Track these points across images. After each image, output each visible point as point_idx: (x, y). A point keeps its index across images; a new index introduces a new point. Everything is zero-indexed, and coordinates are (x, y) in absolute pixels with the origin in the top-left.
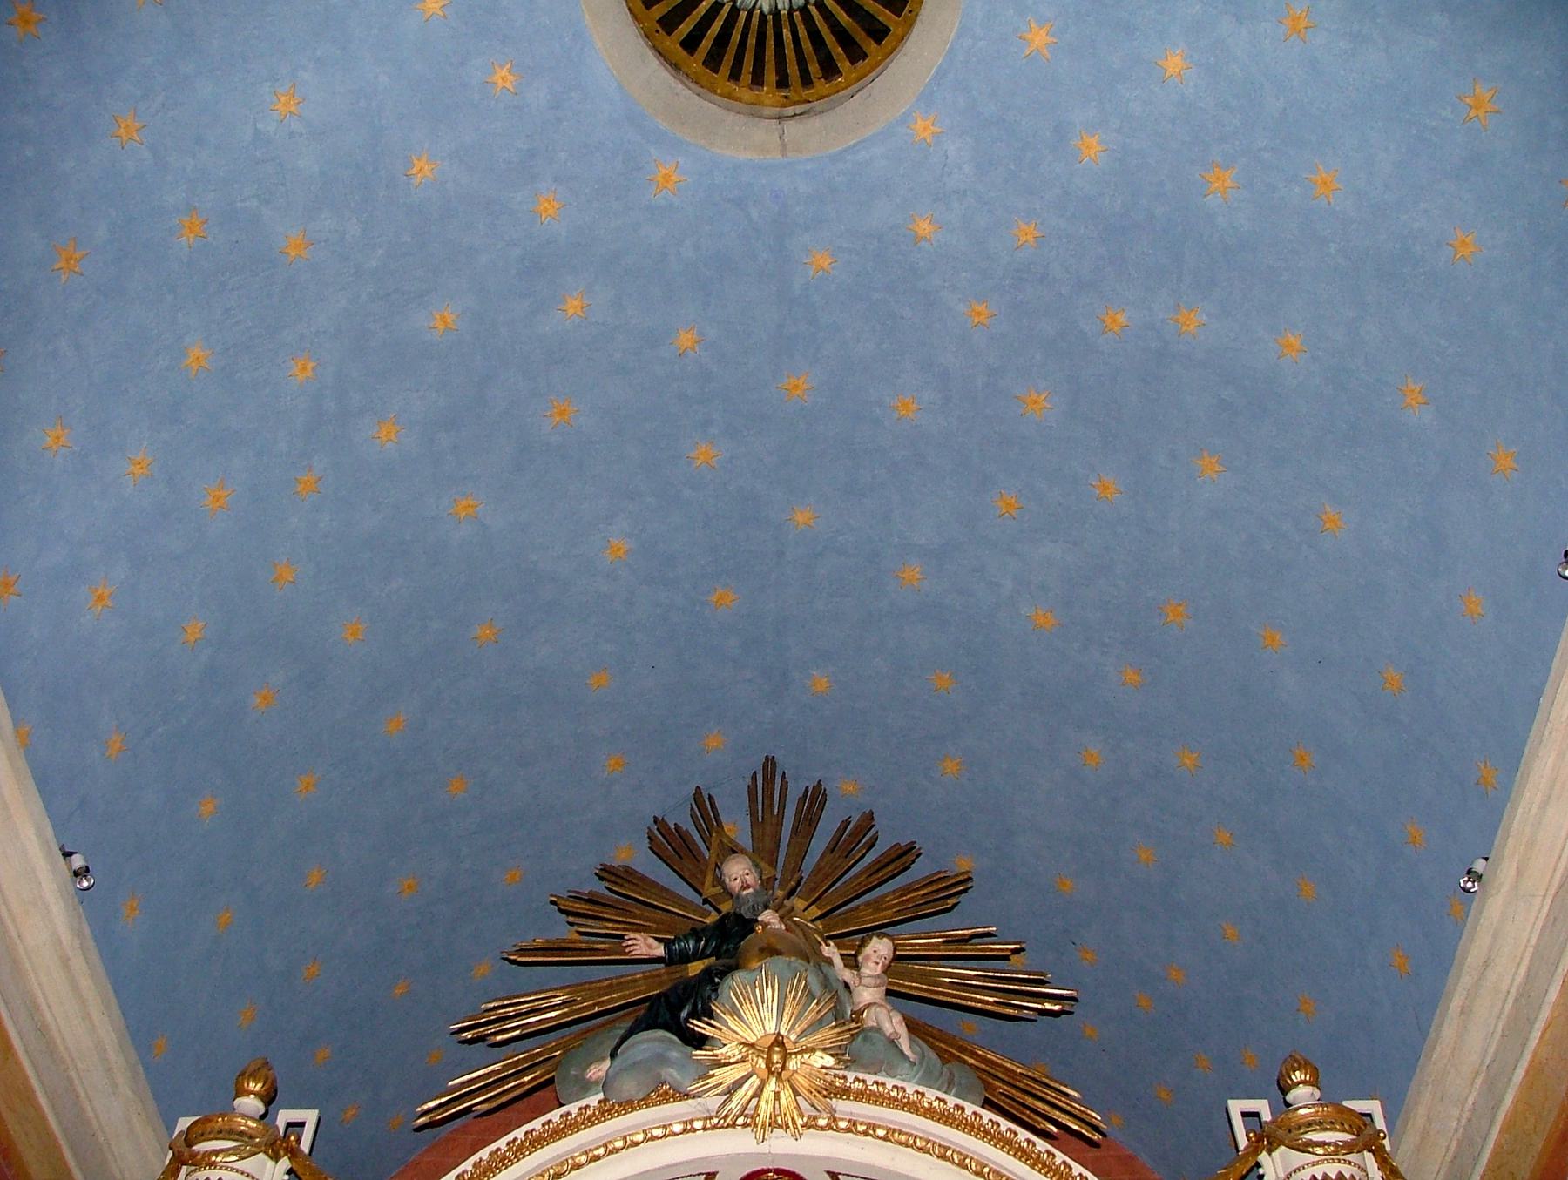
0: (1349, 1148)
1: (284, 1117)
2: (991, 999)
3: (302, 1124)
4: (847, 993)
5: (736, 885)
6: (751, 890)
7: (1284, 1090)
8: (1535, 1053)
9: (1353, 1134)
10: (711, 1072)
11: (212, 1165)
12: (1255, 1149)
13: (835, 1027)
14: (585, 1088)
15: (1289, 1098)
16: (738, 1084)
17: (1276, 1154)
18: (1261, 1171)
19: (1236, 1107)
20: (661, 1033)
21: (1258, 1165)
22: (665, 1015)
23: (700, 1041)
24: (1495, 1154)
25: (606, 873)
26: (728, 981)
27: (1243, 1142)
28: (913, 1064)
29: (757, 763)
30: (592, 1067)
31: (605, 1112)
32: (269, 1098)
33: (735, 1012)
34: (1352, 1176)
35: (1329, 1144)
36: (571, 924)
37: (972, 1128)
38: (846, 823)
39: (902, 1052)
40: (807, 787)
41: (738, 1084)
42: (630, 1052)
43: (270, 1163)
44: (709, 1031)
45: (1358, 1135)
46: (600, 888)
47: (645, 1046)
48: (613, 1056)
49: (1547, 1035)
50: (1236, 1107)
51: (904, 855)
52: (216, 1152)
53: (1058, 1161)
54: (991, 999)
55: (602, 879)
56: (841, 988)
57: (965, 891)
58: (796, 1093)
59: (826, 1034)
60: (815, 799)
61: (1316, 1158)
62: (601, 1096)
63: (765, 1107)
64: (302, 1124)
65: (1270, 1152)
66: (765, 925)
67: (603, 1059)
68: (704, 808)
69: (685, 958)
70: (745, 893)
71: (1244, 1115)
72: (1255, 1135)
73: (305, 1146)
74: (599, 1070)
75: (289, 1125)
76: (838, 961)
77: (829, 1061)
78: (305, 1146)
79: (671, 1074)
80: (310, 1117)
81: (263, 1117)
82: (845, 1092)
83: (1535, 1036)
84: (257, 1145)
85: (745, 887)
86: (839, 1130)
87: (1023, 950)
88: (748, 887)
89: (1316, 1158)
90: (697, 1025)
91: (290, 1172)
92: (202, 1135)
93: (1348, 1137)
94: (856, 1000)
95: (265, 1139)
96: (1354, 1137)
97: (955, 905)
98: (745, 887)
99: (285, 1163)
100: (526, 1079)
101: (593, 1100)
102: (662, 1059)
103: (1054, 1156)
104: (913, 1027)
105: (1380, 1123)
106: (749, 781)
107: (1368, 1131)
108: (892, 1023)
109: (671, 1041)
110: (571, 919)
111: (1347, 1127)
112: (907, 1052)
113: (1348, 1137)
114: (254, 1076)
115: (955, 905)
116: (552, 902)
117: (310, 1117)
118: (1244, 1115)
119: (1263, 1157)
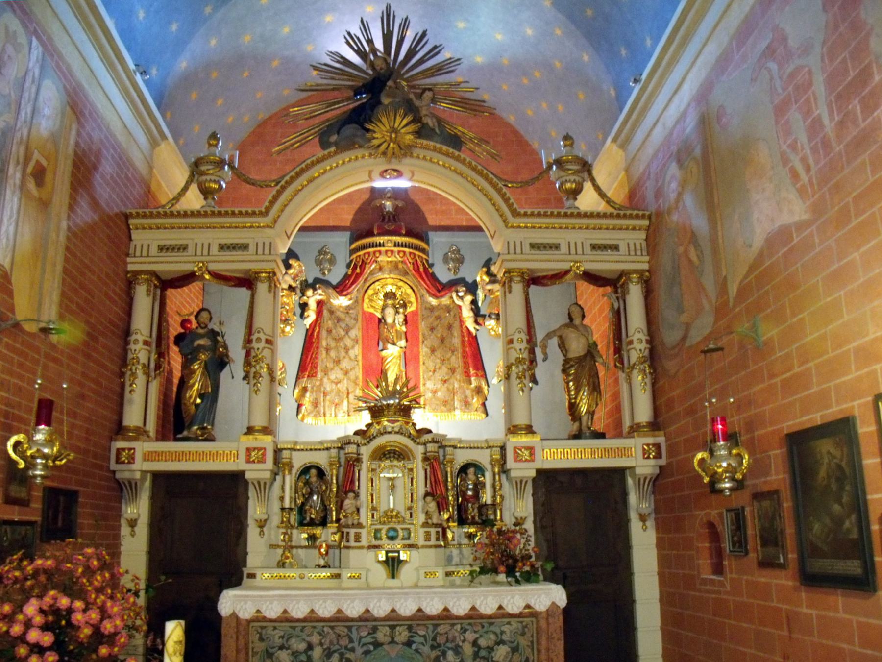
11: (208, 174)
16: (379, 146)
23: (368, 130)
41: (379, 146)
44: (371, 128)
48: (338, 133)
52: (208, 170)
63: (390, 151)
77: (412, 137)
90: (367, 126)
98: (381, 69)
102: (355, 136)
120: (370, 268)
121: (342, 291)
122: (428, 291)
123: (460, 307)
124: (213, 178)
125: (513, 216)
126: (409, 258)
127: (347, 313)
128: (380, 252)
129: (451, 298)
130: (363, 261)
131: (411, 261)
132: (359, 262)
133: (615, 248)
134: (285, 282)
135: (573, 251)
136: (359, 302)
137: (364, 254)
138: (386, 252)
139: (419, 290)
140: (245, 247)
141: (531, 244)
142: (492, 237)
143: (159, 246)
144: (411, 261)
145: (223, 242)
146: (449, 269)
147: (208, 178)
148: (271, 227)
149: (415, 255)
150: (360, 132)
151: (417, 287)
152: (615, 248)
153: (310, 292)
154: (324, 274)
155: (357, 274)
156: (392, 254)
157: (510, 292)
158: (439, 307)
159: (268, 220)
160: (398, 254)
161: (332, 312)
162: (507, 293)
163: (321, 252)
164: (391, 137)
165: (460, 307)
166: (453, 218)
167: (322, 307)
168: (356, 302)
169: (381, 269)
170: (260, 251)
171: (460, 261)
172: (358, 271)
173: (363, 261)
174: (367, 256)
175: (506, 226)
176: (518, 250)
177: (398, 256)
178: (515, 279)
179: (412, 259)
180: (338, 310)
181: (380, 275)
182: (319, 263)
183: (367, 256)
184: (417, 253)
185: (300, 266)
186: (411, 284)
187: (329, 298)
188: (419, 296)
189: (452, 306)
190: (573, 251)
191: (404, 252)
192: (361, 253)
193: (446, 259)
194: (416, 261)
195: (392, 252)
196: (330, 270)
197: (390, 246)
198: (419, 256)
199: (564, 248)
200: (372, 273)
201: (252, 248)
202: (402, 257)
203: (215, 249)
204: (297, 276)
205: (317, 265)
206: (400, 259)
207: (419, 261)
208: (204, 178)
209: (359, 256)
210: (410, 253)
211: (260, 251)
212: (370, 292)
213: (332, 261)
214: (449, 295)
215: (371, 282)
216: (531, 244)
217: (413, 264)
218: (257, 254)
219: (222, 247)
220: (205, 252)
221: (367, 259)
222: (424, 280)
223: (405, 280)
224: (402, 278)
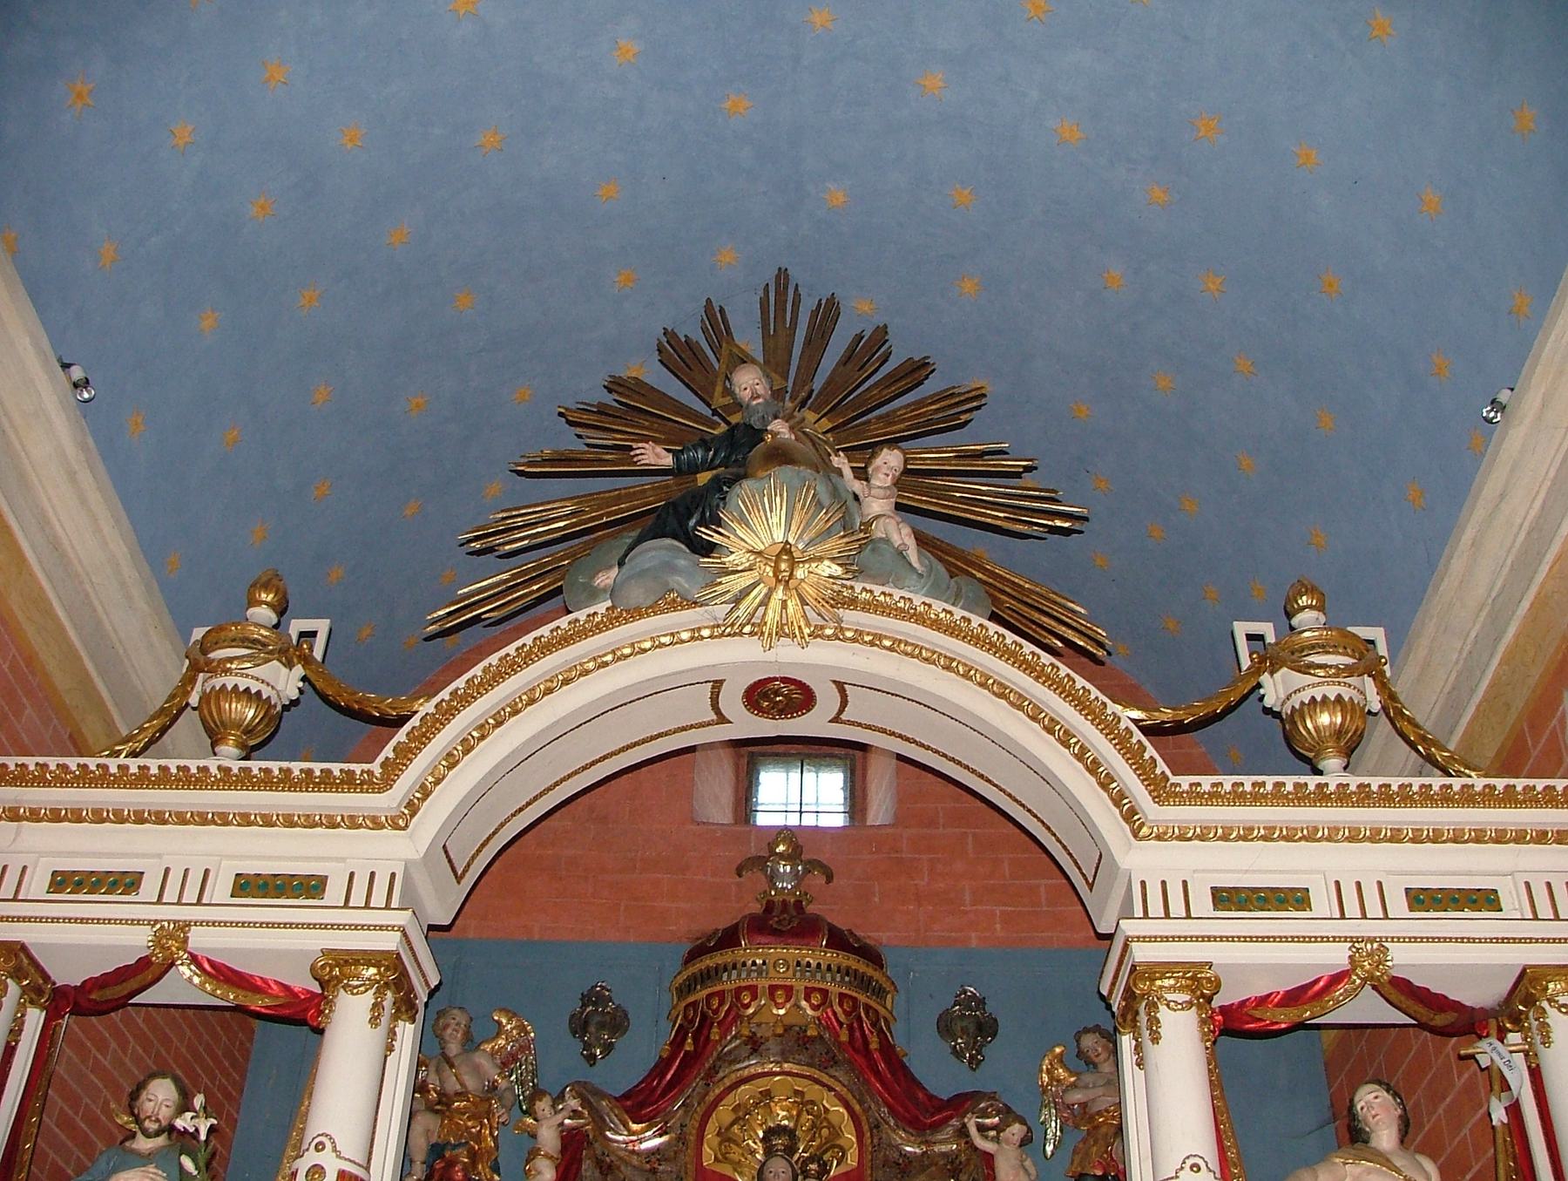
0: (1350, 671)
1: (296, 626)
2: (1002, 515)
3: (313, 634)
4: (856, 504)
5: (746, 395)
6: (760, 400)
7: (1289, 616)
8: (1543, 585)
9: (1355, 658)
10: (719, 580)
11: (227, 671)
12: (1257, 670)
13: (844, 537)
14: (593, 595)
15: (1295, 621)
16: (746, 592)
17: (1277, 675)
18: (1262, 691)
19: (1241, 629)
20: (668, 541)
21: (1259, 686)
22: (672, 523)
23: (708, 549)
24: (1492, 686)
25: (616, 384)
26: (737, 489)
27: (1246, 663)
28: (921, 576)
29: (769, 275)
30: (600, 575)
31: (612, 620)
32: (282, 609)
33: (743, 521)
34: (1351, 698)
35: (1331, 667)
36: (579, 436)
37: (978, 640)
38: (860, 337)
39: (910, 564)
40: (820, 300)
41: (746, 592)
42: (638, 560)
43: (284, 670)
44: (716, 539)
45: (1360, 659)
46: (609, 399)
47: (653, 553)
48: (621, 564)
49: (1555, 568)
50: (1241, 629)
51: (917, 371)
52: (231, 660)
53: (1062, 674)
54: (1002, 515)
55: (610, 391)
56: (851, 497)
57: (978, 408)
58: (804, 602)
59: (834, 544)
60: (828, 313)
61: (1318, 680)
62: (609, 603)
63: (772, 615)
64: (313, 634)
65: (1272, 674)
66: (774, 434)
67: (611, 567)
68: (716, 321)
69: (694, 468)
70: (755, 403)
71: (1250, 637)
72: (1259, 657)
73: (318, 654)
74: (606, 579)
75: (302, 635)
76: (848, 472)
77: (837, 570)
78: (318, 654)
79: (679, 581)
80: (322, 626)
81: (276, 626)
82: (852, 603)
83: (1544, 569)
84: (271, 652)
85: (755, 396)
86: (845, 639)
87: (1036, 468)
88: (758, 397)
89: (1318, 680)
90: (705, 533)
91: (304, 679)
92: (216, 643)
93: (1350, 661)
94: (866, 510)
95: (278, 647)
96: (1356, 661)
97: (967, 423)
98: (755, 396)
99: (299, 671)
100: (535, 588)
101: (601, 607)
102: (672, 569)
103: (1058, 669)
104: (922, 541)
105: (1382, 649)
106: (761, 293)
107: (1369, 656)
108: (900, 534)
109: (681, 550)
110: (579, 431)
111: (1349, 651)
112: (916, 564)
113: (1350, 661)
114: (266, 587)
115: (967, 423)
116: (561, 414)
117: (322, 626)
118: (1250, 637)
119: (1265, 678)
120: (723, 1036)
121: (642, 1105)
122: (892, 1111)
123: (988, 1158)
124: (243, 683)
125: (1158, 799)
126: (838, 1009)
127: (654, 1171)
128: (753, 991)
129: (963, 1132)
130: (704, 1017)
131: (842, 1018)
132: (692, 1022)
133: (1486, 900)
134: (477, 1069)
135: (1352, 908)
136: (687, 1142)
137: (709, 997)
138: (773, 989)
139: (867, 1110)
140: (312, 887)
141: (1215, 892)
142: (1091, 886)
143: (55, 873)
144: (842, 1018)
145: (251, 868)
146: (958, 1054)
147: (230, 681)
148: (396, 827)
149: (854, 999)
150: (683, 558)
151: (860, 1102)
152: (1486, 900)
153: (543, 1106)
154: (591, 1059)
155: (687, 1053)
156: (788, 1000)
157: (1156, 1039)
158: (924, 1161)
159: (387, 802)
160: (807, 999)
161: (605, 1168)
162: (1147, 1043)
163: (586, 999)
164: (776, 571)
165: (988, 1158)
166: (966, 913)
167: (579, 1150)
168: (681, 1139)
169: (755, 1045)
170: (358, 898)
171: (986, 1028)
172: (689, 1046)
173: (704, 1016)
174: (715, 1003)
175: (1135, 835)
176: (1177, 907)
177: (804, 1003)
178: (1169, 997)
179: (847, 1014)
180: (627, 1163)
181: (753, 1065)
182: (579, 1026)
183: (715, 1003)
184: (862, 998)
185: (522, 1028)
186: (844, 1091)
187: (601, 1125)
188: (866, 1128)
189: (963, 1158)
190: (1352, 908)
191: (824, 993)
192: (701, 994)
193: (945, 1026)
194: (859, 1019)
195: (789, 991)
196: (608, 1048)
197: (781, 975)
198: (868, 1008)
199: (1322, 902)
200: (732, 1059)
201: (334, 893)
202: (815, 1008)
203: (221, 888)
204: (513, 1057)
205: (574, 1033)
206: (809, 1012)
207: (866, 1025)
208: (218, 682)
209: (694, 1004)
210: (842, 996)
211: (358, 898)
212: (724, 1113)
213: (618, 1023)
214: (954, 1122)
215: (727, 1082)
216: (1215, 892)
217: (851, 1028)
218: (346, 905)
219: (246, 886)
220: (191, 895)
221: (716, 1012)
222: (877, 1073)
223: (825, 1079)
224: (817, 1074)
